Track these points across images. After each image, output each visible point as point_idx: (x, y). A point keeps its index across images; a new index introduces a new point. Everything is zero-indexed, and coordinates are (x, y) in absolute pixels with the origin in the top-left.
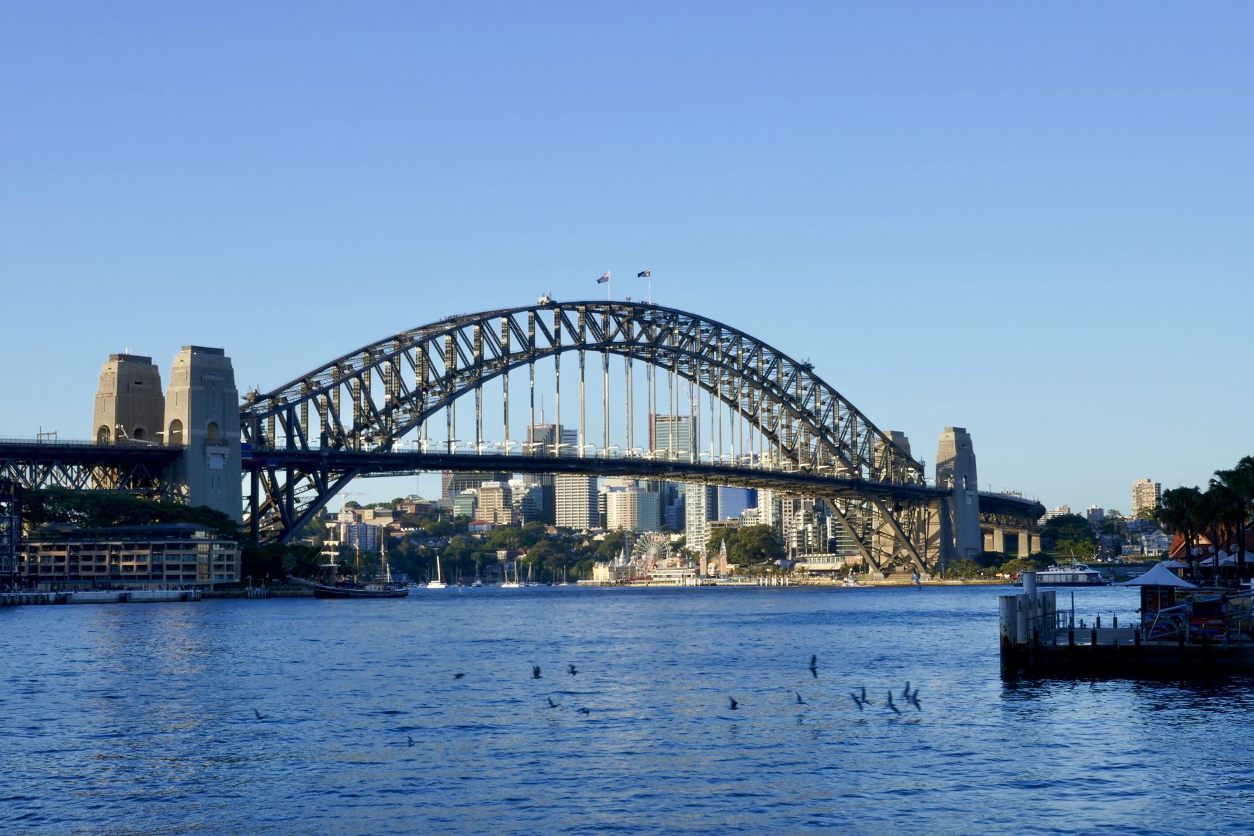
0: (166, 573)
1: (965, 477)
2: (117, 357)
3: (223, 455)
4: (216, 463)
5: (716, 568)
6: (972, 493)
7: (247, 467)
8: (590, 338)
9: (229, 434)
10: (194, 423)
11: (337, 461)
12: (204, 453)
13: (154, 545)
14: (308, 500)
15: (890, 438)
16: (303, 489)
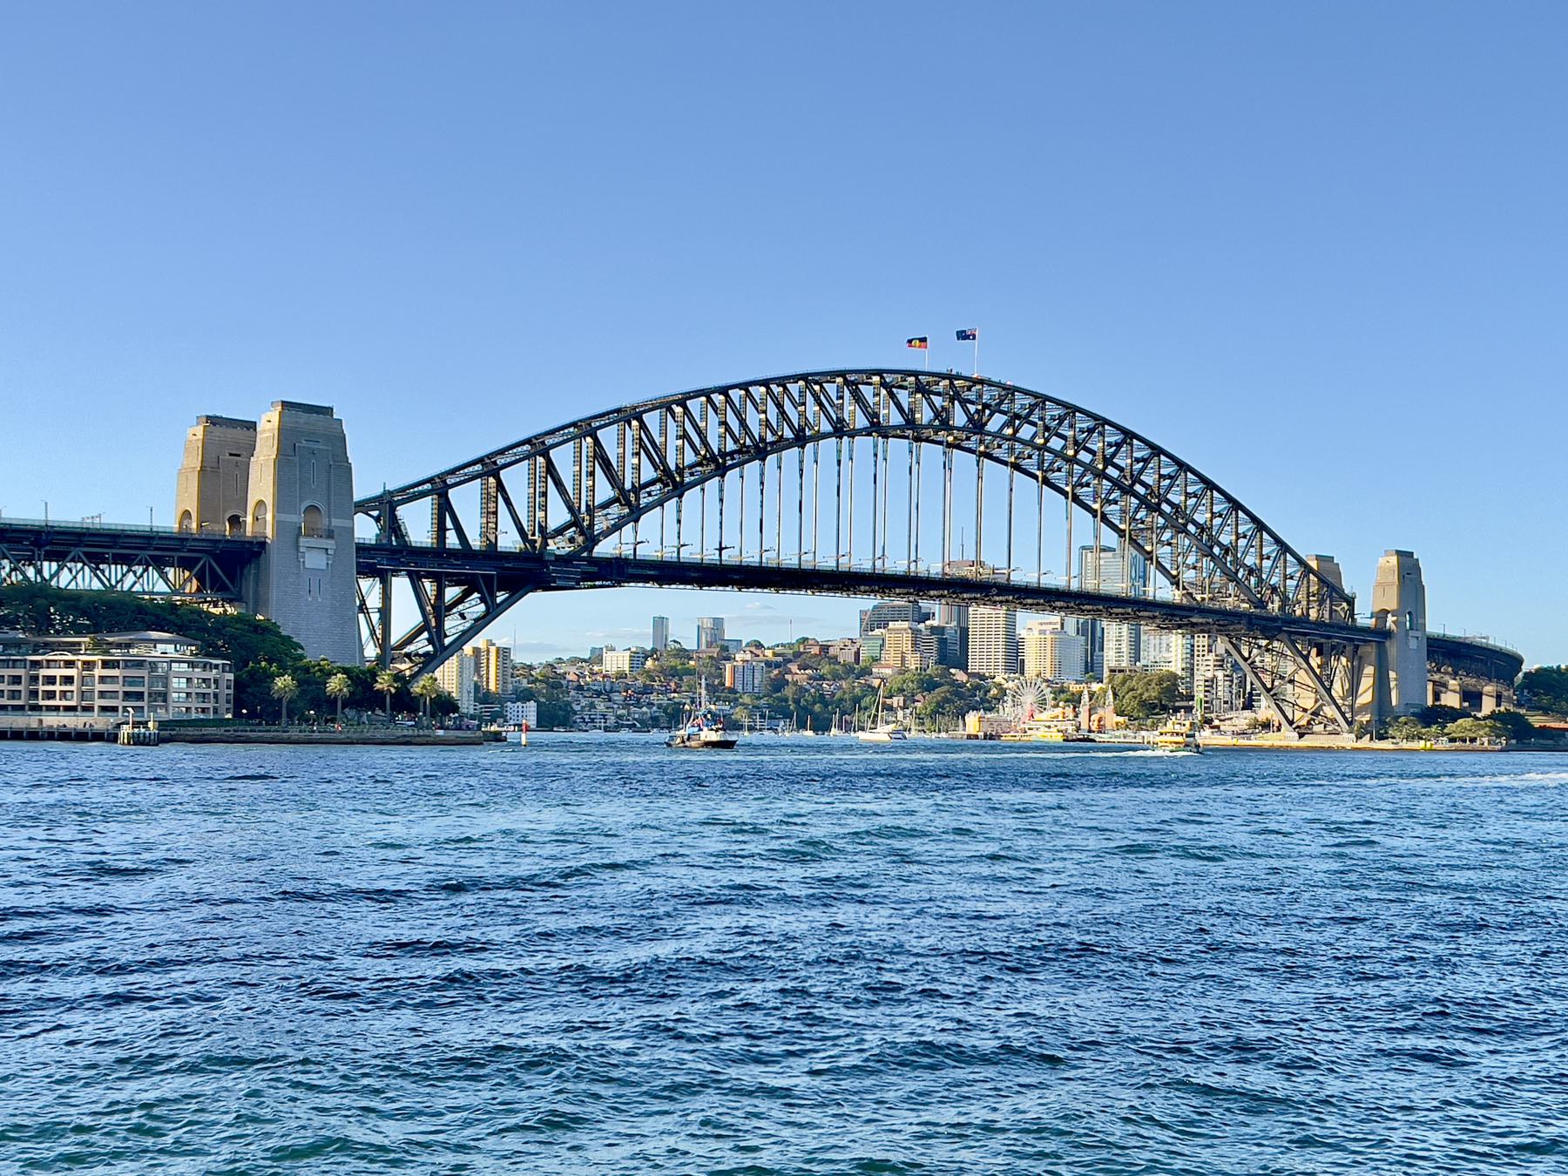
0: (98, 702)
1: (1409, 613)
2: (204, 420)
3: (327, 549)
4: (315, 560)
5: (1099, 721)
6: (1419, 634)
7: (367, 570)
8: (896, 419)
9: (336, 522)
10: (280, 506)
11: (506, 565)
12: (297, 547)
13: (31, 661)
14: (475, 616)
15: (1314, 564)
16: (473, 603)
